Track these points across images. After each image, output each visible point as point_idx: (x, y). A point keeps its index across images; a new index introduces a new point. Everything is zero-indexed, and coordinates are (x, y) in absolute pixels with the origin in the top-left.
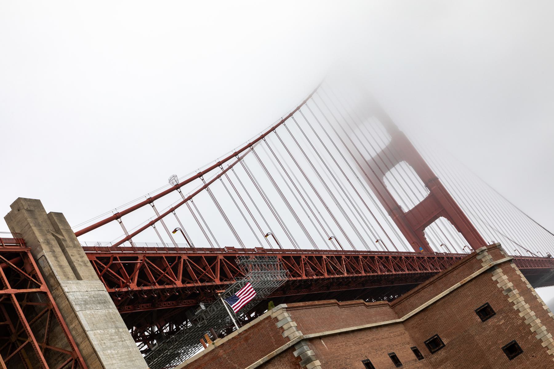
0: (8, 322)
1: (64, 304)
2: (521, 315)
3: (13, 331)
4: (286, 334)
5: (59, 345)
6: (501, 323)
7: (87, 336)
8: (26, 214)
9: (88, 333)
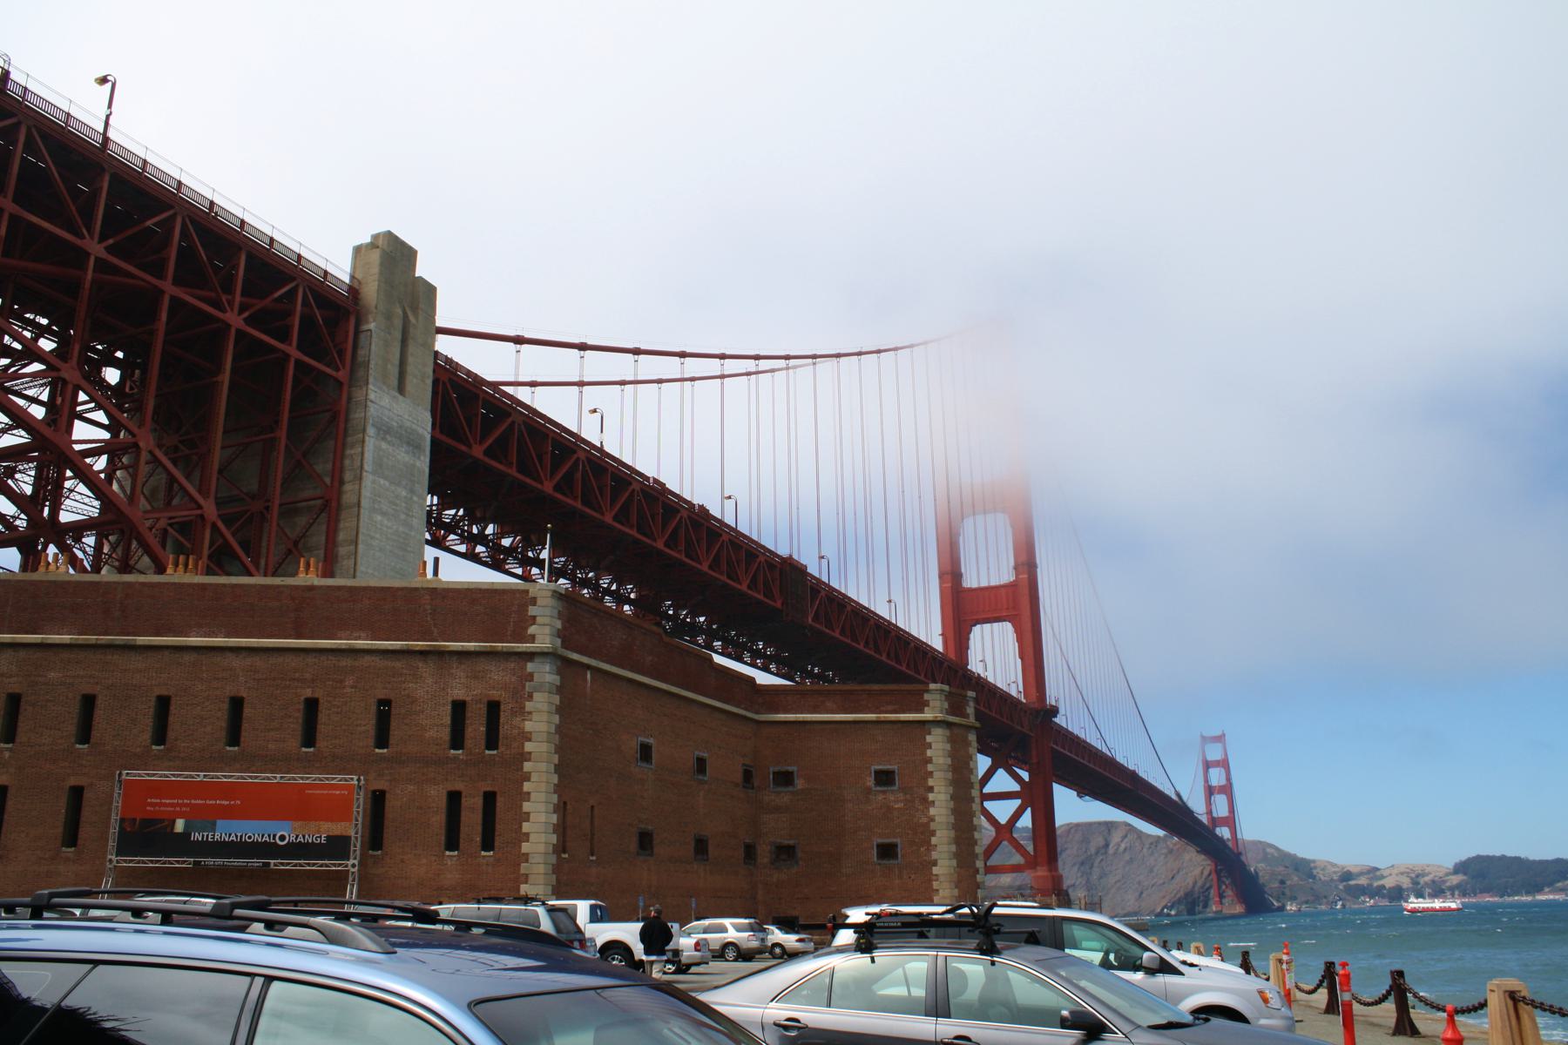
6: (896, 806)
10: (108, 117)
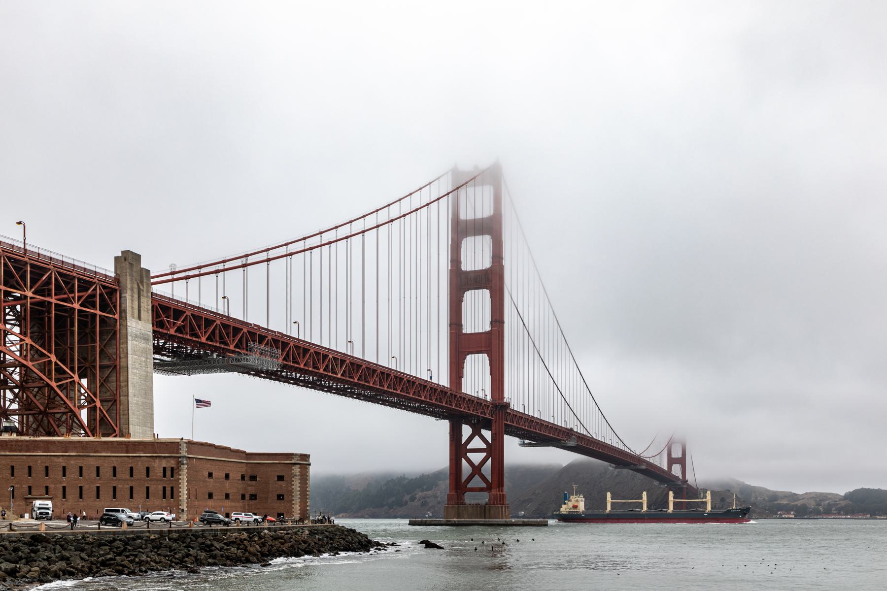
0: (88, 320)
1: (123, 331)
2: (293, 487)
3: (89, 326)
4: (181, 451)
5: (111, 351)
7: (127, 357)
8: (128, 266)
9: (129, 355)
10: (24, 240)
